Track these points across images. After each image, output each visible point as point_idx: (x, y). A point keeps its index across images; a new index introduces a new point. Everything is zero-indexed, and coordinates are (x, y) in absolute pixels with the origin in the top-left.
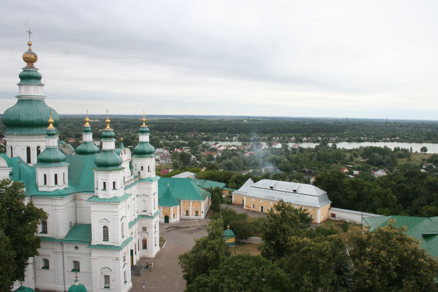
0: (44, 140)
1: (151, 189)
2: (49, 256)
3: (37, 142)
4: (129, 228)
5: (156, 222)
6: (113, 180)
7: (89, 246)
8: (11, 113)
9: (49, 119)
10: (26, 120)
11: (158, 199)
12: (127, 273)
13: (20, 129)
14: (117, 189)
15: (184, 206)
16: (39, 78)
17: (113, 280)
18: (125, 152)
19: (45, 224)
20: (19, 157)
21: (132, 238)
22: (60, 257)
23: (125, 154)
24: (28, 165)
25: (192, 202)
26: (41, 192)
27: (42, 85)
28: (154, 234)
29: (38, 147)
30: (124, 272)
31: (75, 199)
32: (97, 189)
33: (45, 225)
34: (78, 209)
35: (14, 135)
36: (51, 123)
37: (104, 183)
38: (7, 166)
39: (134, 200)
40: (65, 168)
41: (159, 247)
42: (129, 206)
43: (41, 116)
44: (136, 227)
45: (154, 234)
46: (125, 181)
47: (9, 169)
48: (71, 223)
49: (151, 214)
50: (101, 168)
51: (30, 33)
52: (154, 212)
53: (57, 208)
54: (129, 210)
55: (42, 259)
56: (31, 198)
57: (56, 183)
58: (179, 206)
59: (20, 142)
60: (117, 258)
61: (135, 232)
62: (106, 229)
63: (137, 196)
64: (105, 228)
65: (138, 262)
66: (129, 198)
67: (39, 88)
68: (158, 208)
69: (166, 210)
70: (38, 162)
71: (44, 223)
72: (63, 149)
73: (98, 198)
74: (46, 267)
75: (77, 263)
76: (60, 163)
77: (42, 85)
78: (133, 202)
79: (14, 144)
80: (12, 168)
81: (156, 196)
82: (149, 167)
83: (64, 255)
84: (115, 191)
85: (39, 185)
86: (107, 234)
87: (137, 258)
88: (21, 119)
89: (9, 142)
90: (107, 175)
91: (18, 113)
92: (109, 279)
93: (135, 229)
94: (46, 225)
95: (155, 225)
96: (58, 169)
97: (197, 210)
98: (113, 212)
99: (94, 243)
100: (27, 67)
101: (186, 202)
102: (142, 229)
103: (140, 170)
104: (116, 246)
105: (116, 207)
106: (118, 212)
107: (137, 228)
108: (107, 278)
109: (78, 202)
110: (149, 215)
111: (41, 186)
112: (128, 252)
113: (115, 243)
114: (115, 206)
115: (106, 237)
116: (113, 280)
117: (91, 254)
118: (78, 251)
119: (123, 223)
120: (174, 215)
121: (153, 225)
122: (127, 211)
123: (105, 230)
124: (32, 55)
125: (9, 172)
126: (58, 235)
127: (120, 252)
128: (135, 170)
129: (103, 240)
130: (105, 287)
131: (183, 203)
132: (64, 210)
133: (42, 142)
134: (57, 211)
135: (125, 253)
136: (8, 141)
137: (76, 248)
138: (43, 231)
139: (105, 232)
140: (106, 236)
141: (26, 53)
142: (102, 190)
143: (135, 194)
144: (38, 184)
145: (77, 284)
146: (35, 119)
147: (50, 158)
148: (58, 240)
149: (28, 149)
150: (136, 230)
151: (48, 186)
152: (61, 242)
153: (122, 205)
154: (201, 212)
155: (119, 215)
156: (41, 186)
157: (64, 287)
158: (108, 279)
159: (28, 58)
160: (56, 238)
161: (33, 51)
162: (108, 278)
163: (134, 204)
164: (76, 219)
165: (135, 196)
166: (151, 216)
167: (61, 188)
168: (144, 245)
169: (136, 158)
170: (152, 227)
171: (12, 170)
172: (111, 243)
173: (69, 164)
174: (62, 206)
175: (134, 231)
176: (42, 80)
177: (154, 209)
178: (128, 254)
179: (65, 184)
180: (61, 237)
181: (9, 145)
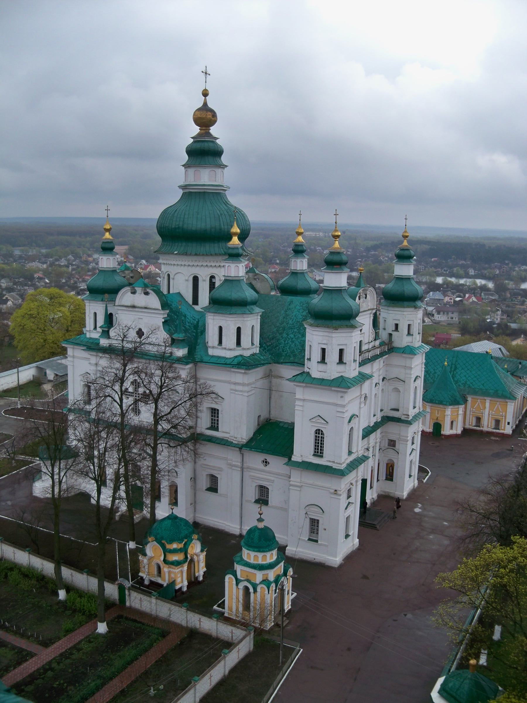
0: (222, 264)
1: (411, 368)
2: (220, 470)
3: (211, 268)
4: (363, 438)
5: (415, 433)
6: (339, 345)
7: (289, 461)
8: (171, 215)
9: (232, 226)
10: (194, 229)
11: (424, 389)
13: (184, 244)
14: (346, 363)
15: (472, 407)
16: (218, 153)
17: (325, 530)
18: (366, 295)
19: (214, 412)
20: (179, 293)
21: (367, 458)
22: (237, 476)
23: (366, 298)
24: (194, 308)
25: (490, 400)
26: (213, 356)
27: (224, 166)
28: (410, 454)
29: (212, 277)
30: (347, 518)
31: (269, 376)
32: (309, 359)
33: (215, 417)
34: (274, 393)
35: (173, 254)
36: (235, 234)
37: (324, 350)
38: (161, 309)
39: (377, 387)
40: (256, 317)
41: (416, 482)
42: (366, 397)
43: (220, 221)
44: (375, 438)
45: (410, 454)
46: (365, 348)
47: (162, 312)
48: (259, 416)
50: (320, 322)
51: (206, 73)
52: (412, 413)
53: (238, 388)
54: (367, 404)
55: (207, 475)
56: (196, 366)
57: (238, 343)
58: (463, 406)
59: (182, 267)
60: (336, 491)
61: (373, 447)
62: (320, 435)
63: (384, 379)
64: (319, 434)
65: (374, 503)
66: (367, 383)
67: (219, 171)
68: (421, 407)
69: (438, 411)
70: (210, 303)
71: (215, 413)
72: (254, 283)
73: (311, 376)
74: (213, 488)
75: (266, 490)
76: (248, 307)
77: (224, 166)
78: (374, 391)
79: (172, 270)
80: (168, 311)
81: (420, 383)
83: (244, 473)
84: (341, 367)
85: (210, 344)
86: (321, 444)
87: (372, 495)
88: (185, 226)
89: (166, 265)
90: (330, 335)
91: (182, 217)
92: (318, 527)
93: (375, 441)
94: (218, 417)
95: (413, 438)
96: (243, 319)
97: (499, 418)
98: (337, 405)
99: (296, 457)
100: (199, 135)
101: (478, 399)
102: (387, 441)
103: (393, 331)
104: (335, 469)
105: (342, 397)
106: (344, 406)
107: (378, 440)
108: (314, 524)
109: (274, 381)
110: (403, 418)
111: (213, 347)
112: (357, 482)
113: (334, 462)
114: (340, 394)
115: (319, 451)
116: (325, 530)
117: (290, 478)
118: (268, 468)
119: (352, 428)
120: (452, 423)
121: (410, 438)
122: (362, 405)
123: (319, 437)
124: (210, 113)
125: (163, 318)
126: (236, 436)
127: (343, 480)
128: (383, 331)
129: (314, 455)
130: (310, 539)
131: (472, 401)
132: (250, 393)
133: (219, 268)
134: (236, 393)
135: (352, 484)
136: (164, 264)
137: (265, 464)
138: (212, 426)
139: (319, 440)
140: (319, 448)
141: (199, 110)
142: (318, 362)
143: (379, 376)
144: (207, 342)
145: (261, 525)
146: (208, 227)
147: (230, 298)
148: (237, 444)
149: (196, 279)
150: (376, 443)
151: (225, 347)
152: (240, 449)
153: (354, 393)
154: (507, 423)
155: (347, 411)
156: (213, 347)
157: (241, 528)
158: (316, 525)
159: (200, 118)
160: (232, 441)
161: (210, 105)
162: (316, 524)
163: (376, 394)
164: (270, 412)
165: (379, 379)
166: (406, 419)
167: (247, 354)
168: (388, 473)
169: (386, 308)
170: (407, 441)
171: (168, 315)
173: (263, 311)
174: (248, 385)
175: (371, 445)
176: (224, 159)
177: (414, 407)
178: (356, 485)
179: (254, 347)
180: (240, 440)
181: (165, 272)
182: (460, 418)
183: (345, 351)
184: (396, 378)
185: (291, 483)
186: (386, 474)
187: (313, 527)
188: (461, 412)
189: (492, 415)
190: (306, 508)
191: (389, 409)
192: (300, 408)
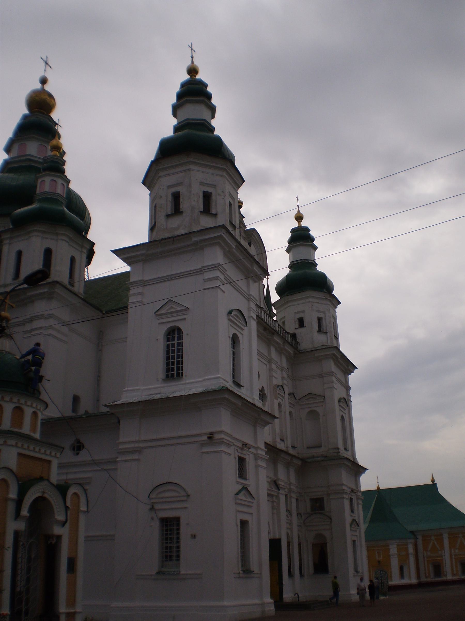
6: (202, 184)
12: (253, 527)
37: (176, 197)
53: (36, 324)
64: (173, 340)
82: (320, 320)
102: (309, 504)
116: (194, 536)
123: (173, 345)
142: (168, 216)
182: (412, 560)
183: (214, 197)
184: (310, 393)
185: (121, 447)
187: (169, 545)
188: (411, 550)
189: (455, 555)
192: (139, 298)
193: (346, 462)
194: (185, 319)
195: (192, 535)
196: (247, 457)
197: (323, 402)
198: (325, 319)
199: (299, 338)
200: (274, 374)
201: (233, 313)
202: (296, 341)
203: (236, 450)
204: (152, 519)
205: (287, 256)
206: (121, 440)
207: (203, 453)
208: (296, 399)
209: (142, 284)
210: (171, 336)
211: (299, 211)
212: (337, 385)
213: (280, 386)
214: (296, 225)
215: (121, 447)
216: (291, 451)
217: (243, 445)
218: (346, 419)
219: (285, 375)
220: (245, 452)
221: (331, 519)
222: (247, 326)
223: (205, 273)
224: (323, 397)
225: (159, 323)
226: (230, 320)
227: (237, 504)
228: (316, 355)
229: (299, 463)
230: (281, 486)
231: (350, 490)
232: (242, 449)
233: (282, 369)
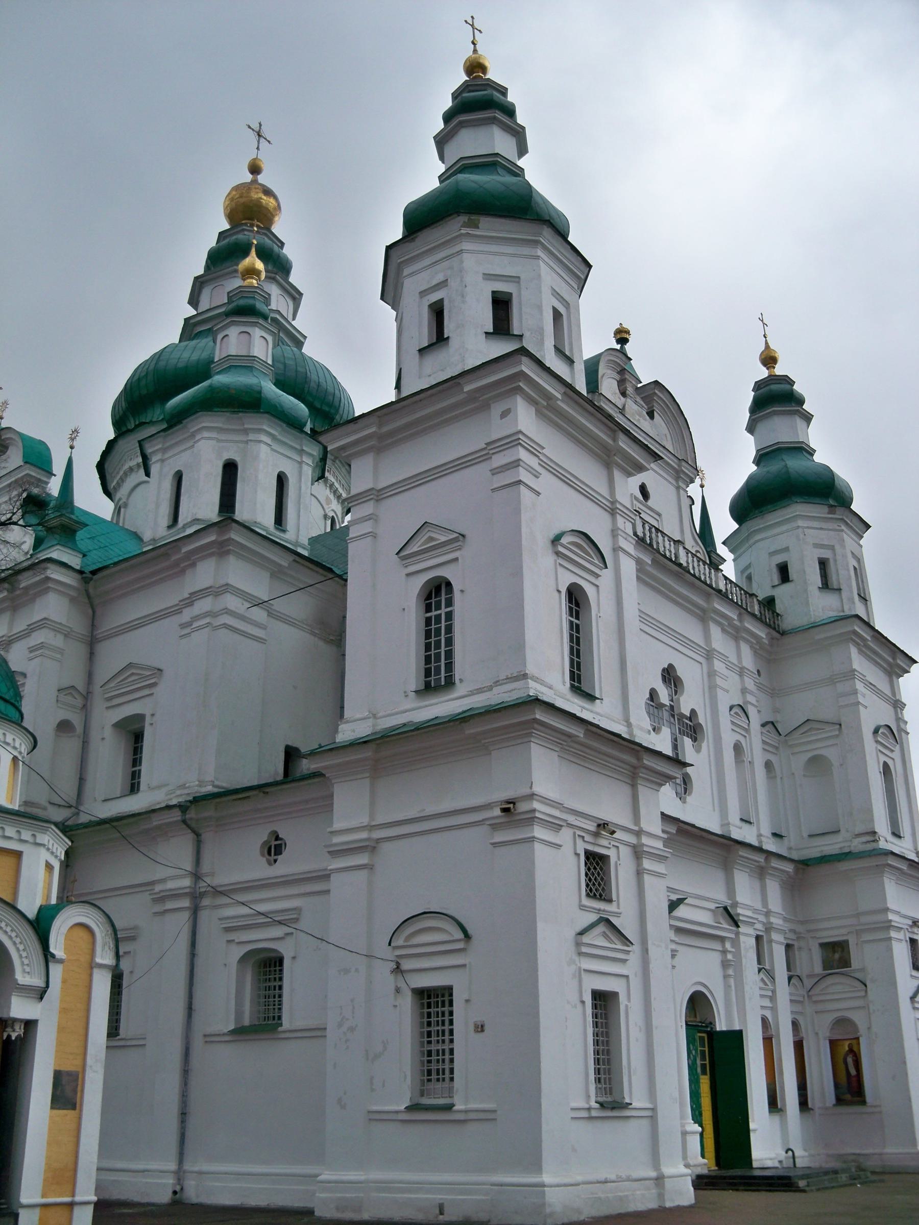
6: (488, 277)
10: (181, 365)
17: (480, 1028)
37: (438, 312)
49: (864, 839)
64: (438, 607)
82: (823, 564)
88: (162, 364)
102: (817, 956)
110: (857, 845)
116: (480, 1028)
123: (438, 617)
172: (472, 693)
186: (837, 1086)
190: (395, 943)
191: (805, 835)
192: (366, 527)
193: (891, 861)
194: (456, 560)
195: (476, 1026)
196: (611, 853)
197: (837, 736)
198: (835, 561)
199: (779, 607)
200: (719, 681)
201: (565, 540)
202: (774, 612)
203: (579, 836)
204: (398, 990)
205: (750, 438)
206: (337, 825)
207: (495, 845)
208: (780, 735)
209: (372, 497)
210: (433, 600)
211: (767, 346)
212: (865, 697)
213: (737, 707)
214: (764, 373)
215: (337, 840)
216: (770, 845)
217: (599, 826)
218: (897, 769)
219: (750, 684)
220: (604, 842)
221: (866, 986)
222: (606, 567)
223: (494, 457)
224: (838, 726)
225: (408, 575)
226: (558, 554)
227: (580, 954)
228: (817, 637)
229: (789, 868)
230: (741, 918)
231: (910, 922)
232: (596, 835)
233: (742, 672)
